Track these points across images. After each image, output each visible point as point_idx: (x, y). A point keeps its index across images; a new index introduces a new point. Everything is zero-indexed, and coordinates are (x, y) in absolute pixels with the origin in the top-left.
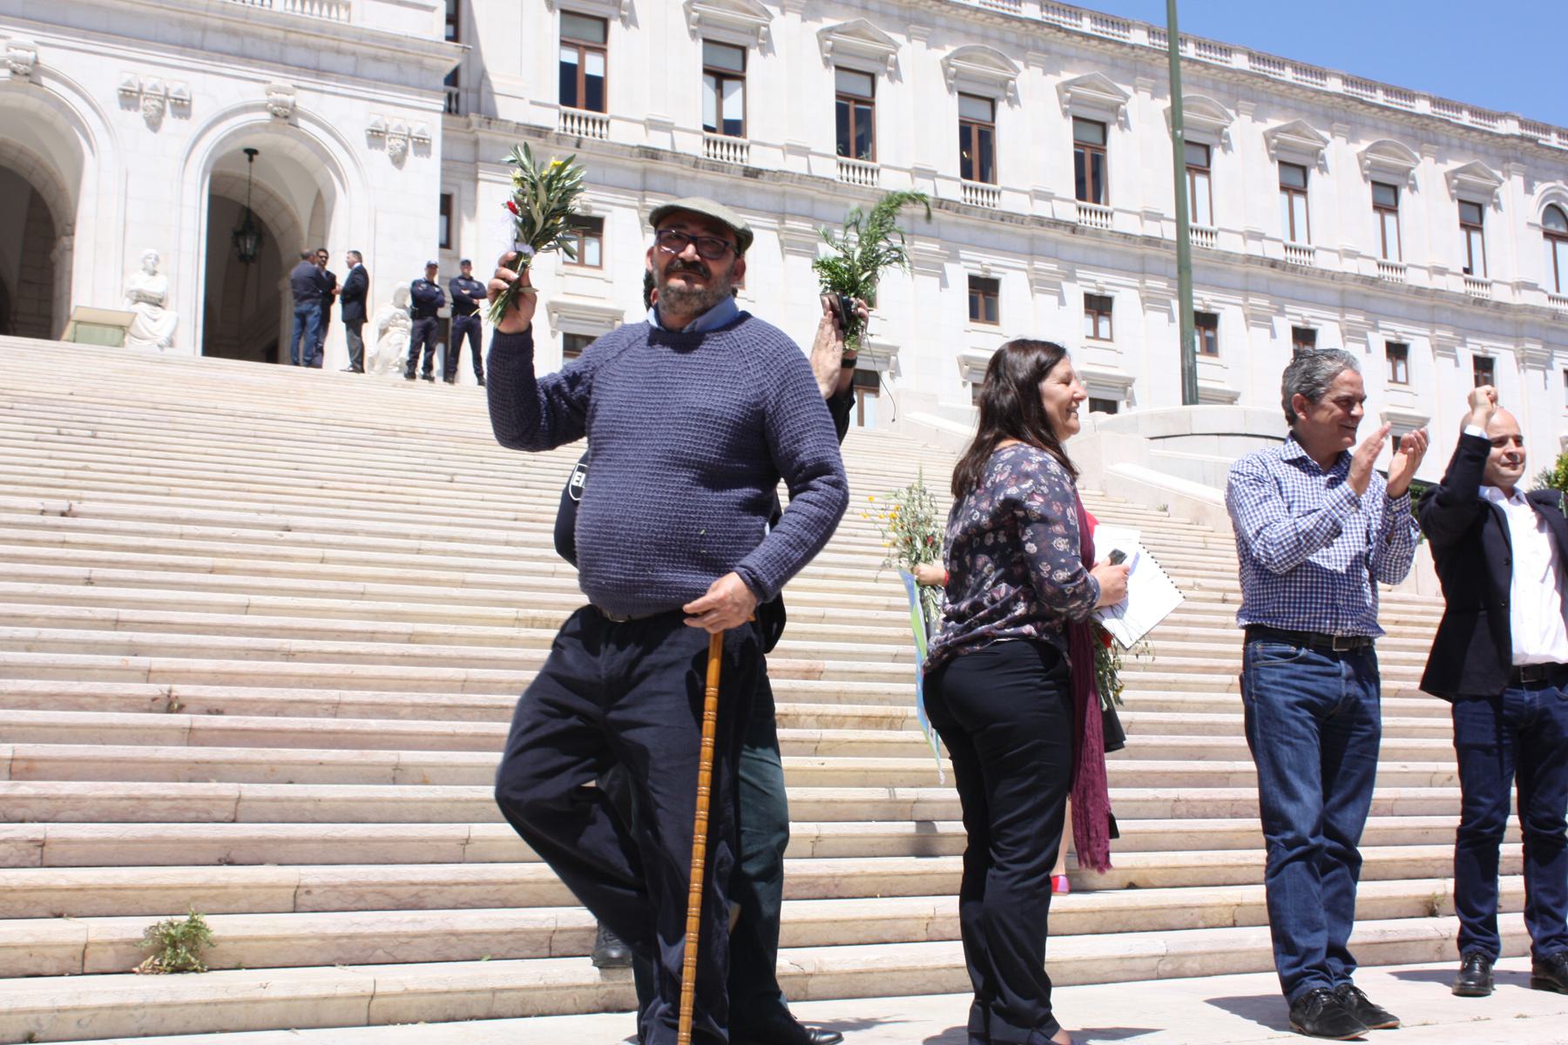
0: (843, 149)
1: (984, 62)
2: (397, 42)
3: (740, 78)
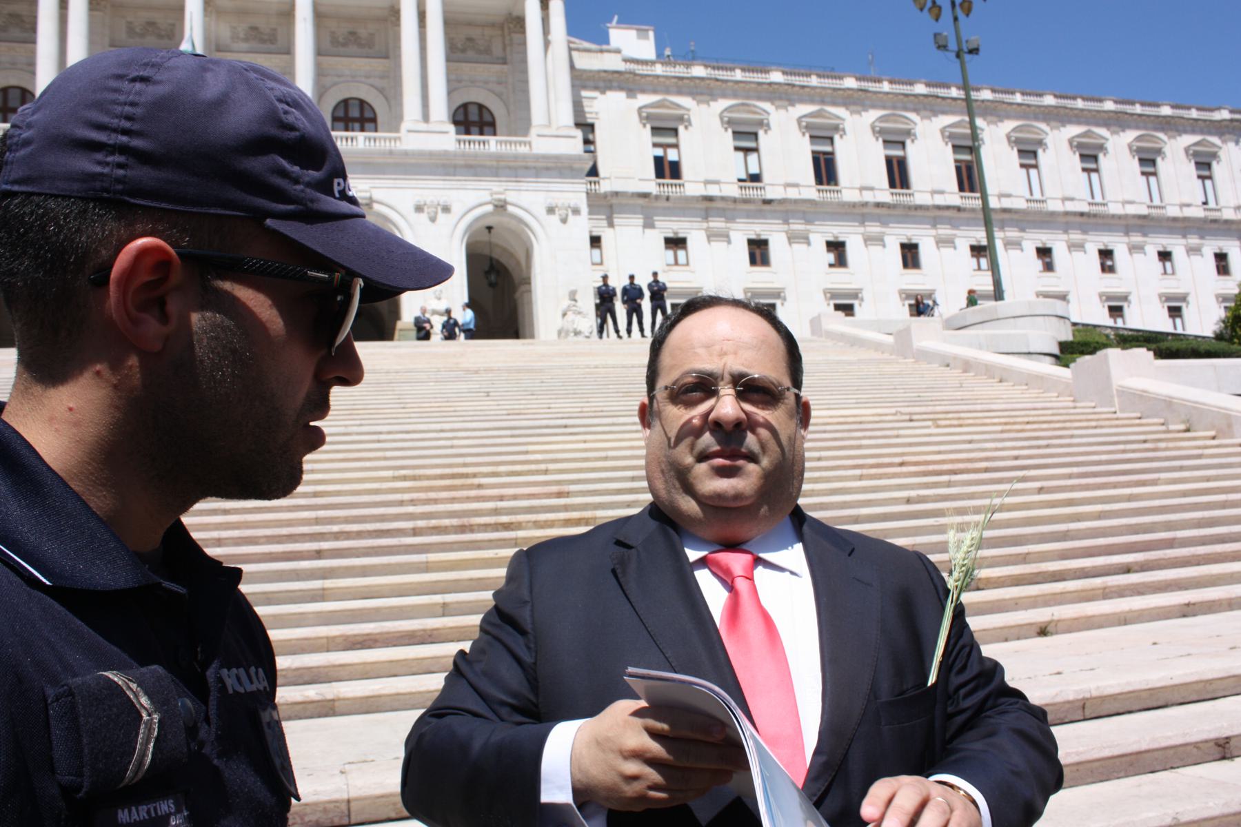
0: (819, 180)
1: (895, 122)
3: (756, 150)
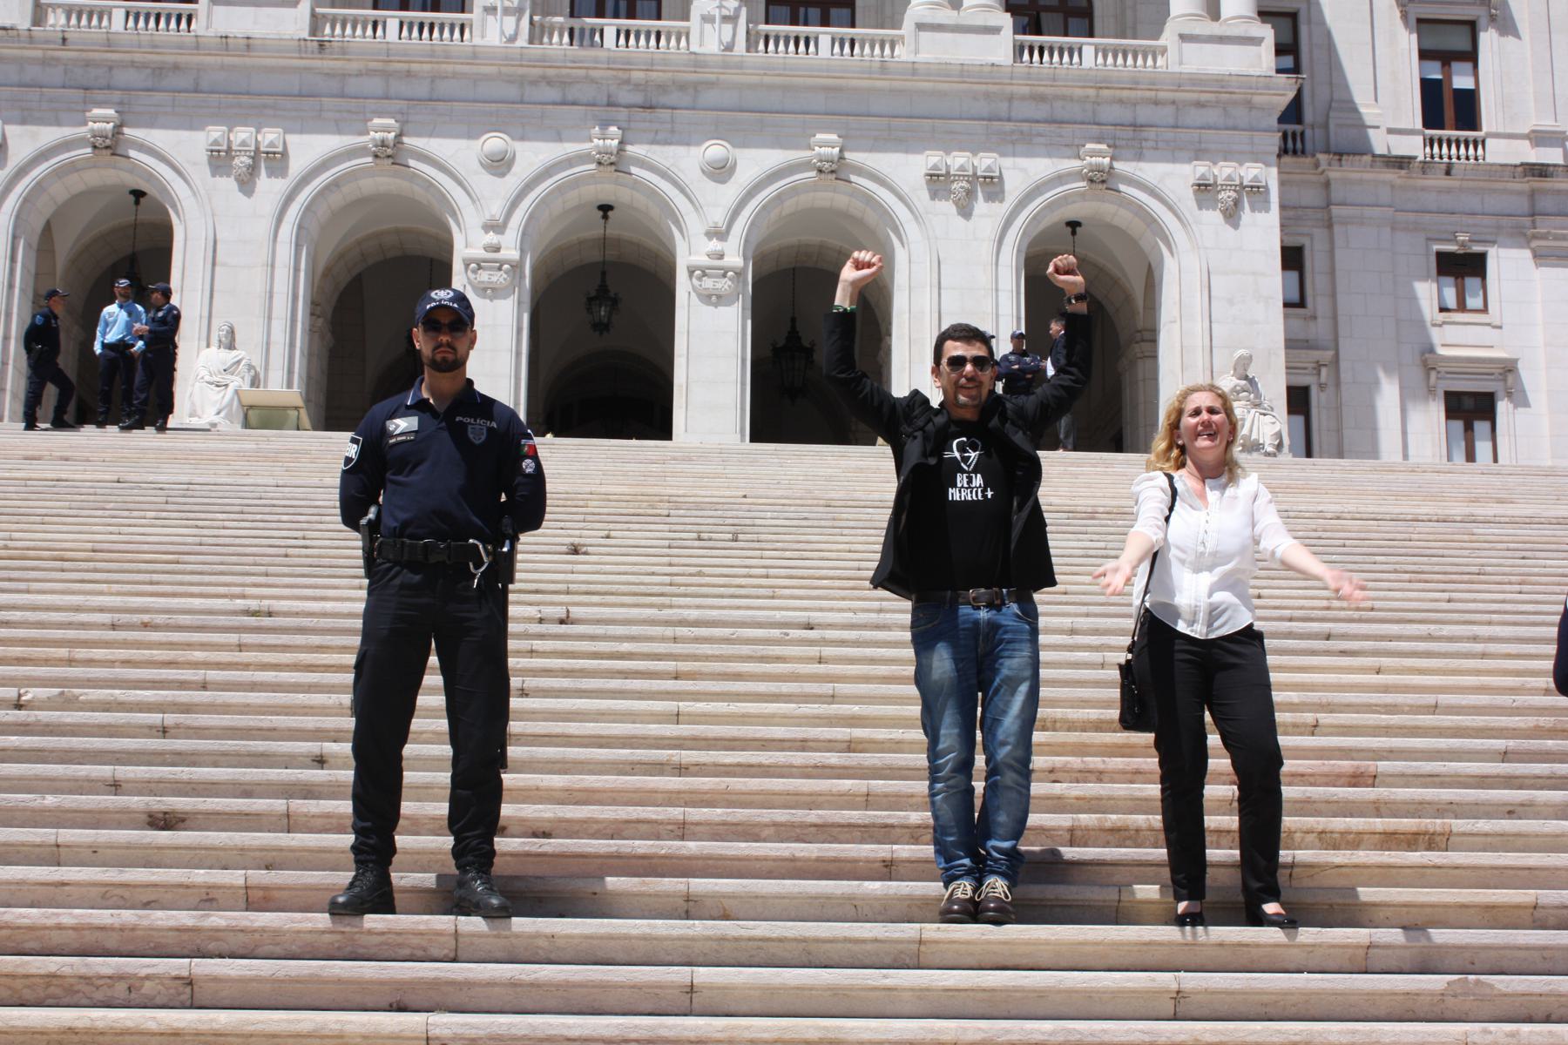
2: (1220, 83)
